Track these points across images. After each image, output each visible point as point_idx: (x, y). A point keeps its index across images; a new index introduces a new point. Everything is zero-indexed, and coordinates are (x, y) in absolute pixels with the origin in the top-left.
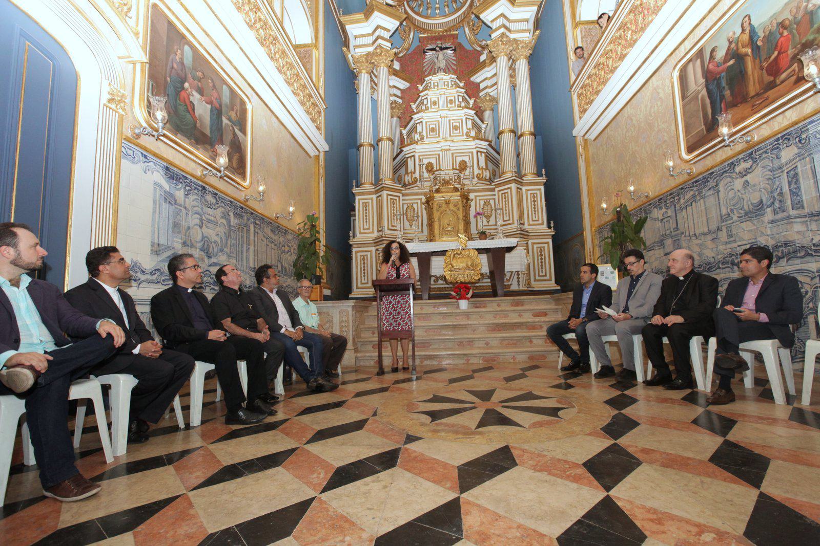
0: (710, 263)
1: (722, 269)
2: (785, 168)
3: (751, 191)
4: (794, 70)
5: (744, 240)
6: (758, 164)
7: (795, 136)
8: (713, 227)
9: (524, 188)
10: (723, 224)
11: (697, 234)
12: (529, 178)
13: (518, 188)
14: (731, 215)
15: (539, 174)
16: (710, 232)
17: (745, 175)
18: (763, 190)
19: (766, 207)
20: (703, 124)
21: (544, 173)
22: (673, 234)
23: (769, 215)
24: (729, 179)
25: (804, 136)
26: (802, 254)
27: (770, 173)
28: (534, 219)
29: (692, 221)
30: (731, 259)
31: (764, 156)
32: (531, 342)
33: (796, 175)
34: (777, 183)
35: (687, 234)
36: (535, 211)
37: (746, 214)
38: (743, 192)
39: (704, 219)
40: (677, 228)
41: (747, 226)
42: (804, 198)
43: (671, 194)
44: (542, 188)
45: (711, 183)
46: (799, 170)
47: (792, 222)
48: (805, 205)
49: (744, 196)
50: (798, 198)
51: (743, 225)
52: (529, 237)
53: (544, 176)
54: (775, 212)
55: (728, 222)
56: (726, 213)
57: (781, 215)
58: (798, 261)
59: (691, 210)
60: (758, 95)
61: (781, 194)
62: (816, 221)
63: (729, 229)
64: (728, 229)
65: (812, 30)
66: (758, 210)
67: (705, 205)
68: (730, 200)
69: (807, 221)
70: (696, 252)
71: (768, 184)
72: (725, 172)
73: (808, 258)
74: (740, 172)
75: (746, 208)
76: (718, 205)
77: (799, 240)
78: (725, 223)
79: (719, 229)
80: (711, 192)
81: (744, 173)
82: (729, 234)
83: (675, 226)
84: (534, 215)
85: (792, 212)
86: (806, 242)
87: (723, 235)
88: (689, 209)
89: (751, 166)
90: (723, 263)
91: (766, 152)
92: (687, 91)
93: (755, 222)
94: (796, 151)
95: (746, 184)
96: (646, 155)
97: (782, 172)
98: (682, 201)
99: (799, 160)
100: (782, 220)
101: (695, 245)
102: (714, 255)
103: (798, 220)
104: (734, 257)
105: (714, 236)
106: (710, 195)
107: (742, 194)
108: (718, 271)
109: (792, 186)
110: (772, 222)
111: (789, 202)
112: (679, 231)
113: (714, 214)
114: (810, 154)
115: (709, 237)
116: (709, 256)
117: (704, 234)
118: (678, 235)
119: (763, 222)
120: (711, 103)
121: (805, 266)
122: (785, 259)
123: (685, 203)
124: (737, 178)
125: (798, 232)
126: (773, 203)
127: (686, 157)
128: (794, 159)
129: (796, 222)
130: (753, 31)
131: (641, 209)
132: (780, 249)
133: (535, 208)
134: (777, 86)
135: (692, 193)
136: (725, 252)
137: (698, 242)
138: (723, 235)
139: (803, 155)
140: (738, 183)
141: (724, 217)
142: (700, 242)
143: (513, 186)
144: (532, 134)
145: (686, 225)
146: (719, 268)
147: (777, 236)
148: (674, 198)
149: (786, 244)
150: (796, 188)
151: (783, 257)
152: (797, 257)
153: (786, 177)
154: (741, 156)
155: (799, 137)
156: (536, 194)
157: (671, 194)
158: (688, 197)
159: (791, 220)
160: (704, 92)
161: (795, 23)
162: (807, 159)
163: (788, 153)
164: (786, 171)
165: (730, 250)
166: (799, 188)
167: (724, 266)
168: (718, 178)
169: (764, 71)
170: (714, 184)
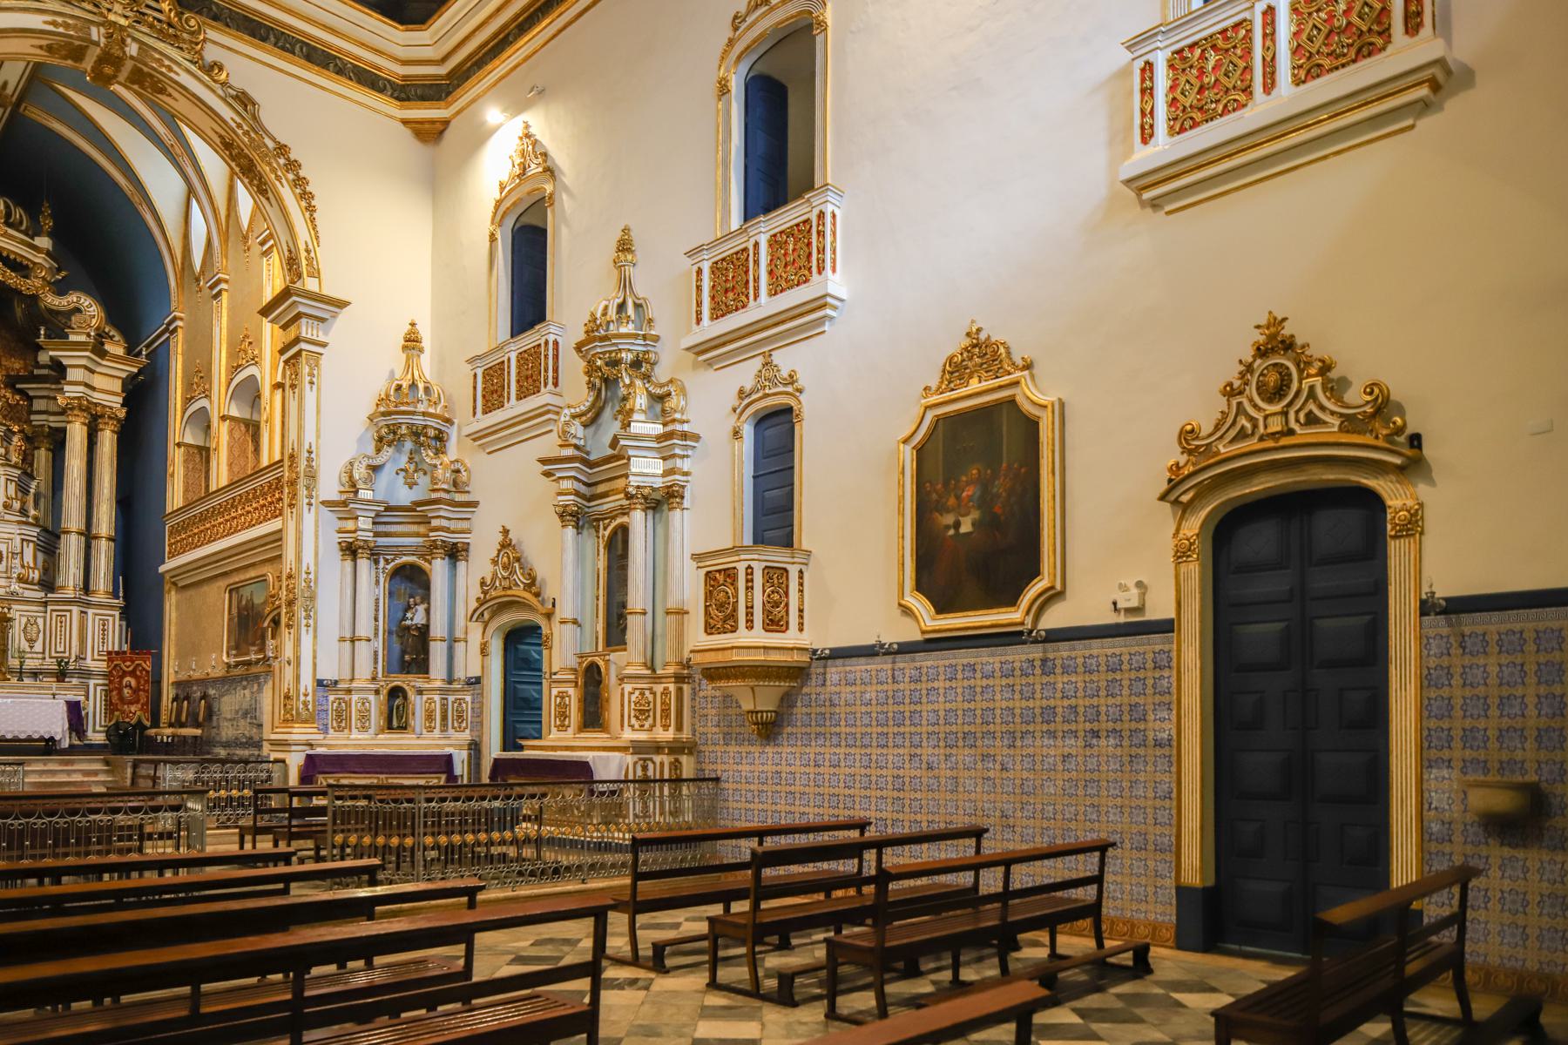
9: (90, 612)
12: (100, 597)
13: (82, 612)
36: (103, 643)
44: (117, 614)
133: (103, 639)
143: (75, 610)
144: (110, 539)
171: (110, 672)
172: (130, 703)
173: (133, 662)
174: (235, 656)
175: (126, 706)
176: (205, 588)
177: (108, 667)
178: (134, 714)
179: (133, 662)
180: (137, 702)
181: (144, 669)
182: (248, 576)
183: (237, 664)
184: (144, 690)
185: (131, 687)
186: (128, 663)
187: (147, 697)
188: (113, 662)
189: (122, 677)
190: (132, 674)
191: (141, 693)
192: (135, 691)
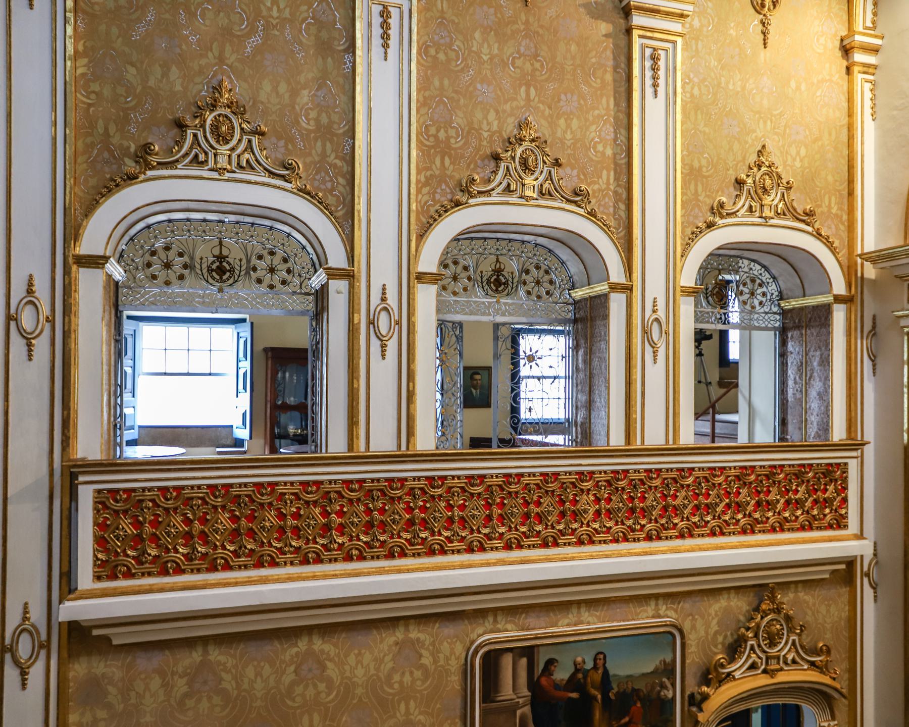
130: (606, 672)
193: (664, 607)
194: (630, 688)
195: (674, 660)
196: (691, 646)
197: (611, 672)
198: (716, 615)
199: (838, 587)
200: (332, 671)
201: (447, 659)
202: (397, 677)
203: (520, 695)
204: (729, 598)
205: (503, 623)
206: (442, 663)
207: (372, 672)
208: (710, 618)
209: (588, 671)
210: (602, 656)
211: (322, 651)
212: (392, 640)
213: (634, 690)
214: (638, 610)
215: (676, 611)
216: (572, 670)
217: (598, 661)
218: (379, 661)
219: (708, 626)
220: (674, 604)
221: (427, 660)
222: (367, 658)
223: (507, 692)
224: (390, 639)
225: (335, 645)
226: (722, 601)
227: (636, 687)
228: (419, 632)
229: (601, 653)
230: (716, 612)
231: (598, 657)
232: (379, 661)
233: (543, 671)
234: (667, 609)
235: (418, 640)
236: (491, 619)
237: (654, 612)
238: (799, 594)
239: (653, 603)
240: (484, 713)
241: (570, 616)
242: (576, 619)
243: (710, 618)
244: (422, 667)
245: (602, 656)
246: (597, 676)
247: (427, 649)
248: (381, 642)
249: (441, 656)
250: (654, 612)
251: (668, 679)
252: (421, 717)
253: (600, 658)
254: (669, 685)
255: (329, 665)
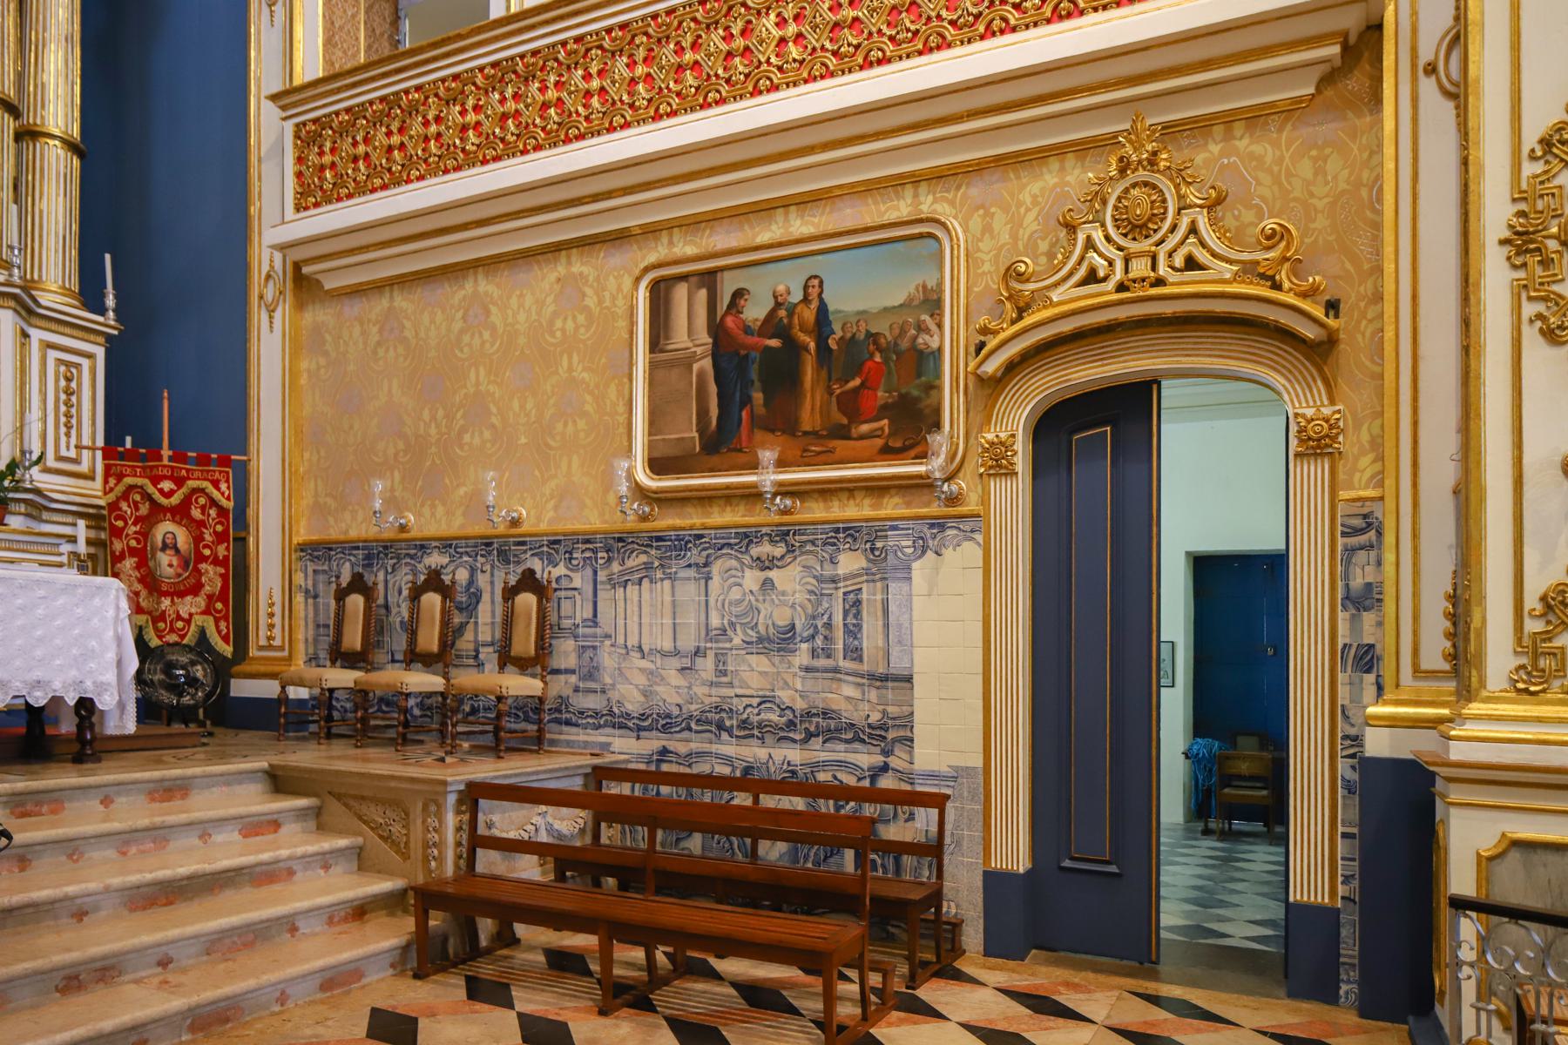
0: (668, 716)
1: (697, 732)
2: (841, 584)
3: (777, 602)
4: (882, 429)
5: (749, 687)
6: (795, 558)
7: (866, 538)
8: (688, 642)
10: (709, 645)
11: (646, 648)
14: (729, 632)
15: (90, 296)
16: (676, 653)
17: (768, 568)
18: (799, 608)
19: (799, 639)
20: (694, 428)
21: (110, 301)
22: (581, 631)
23: (802, 656)
24: (734, 563)
25: (879, 545)
26: (850, 735)
27: (814, 582)
28: (64, 453)
29: (636, 619)
30: (717, 717)
31: (809, 547)
32: (293, 929)
33: (858, 603)
34: (826, 605)
35: (621, 640)
36: (68, 427)
37: (760, 640)
38: (761, 598)
39: (668, 621)
40: (594, 621)
41: (760, 663)
42: (865, 645)
43: (588, 541)
44: (100, 352)
45: (694, 555)
46: (864, 596)
47: (840, 680)
48: (865, 658)
49: (760, 606)
50: (856, 643)
51: (753, 659)
52: (45, 515)
53: (111, 314)
54: (814, 653)
55: (721, 645)
56: (719, 626)
57: (822, 662)
58: (842, 747)
59: (636, 592)
60: (815, 434)
61: (828, 625)
62: (878, 688)
63: (720, 658)
64: (721, 657)
65: (917, 381)
66: (784, 640)
67: (673, 595)
68: (730, 604)
69: (863, 685)
70: (637, 686)
71: (809, 600)
72: (729, 545)
73: (857, 745)
74: (758, 559)
75: (761, 628)
76: (703, 604)
77: (851, 714)
78: (714, 645)
79: (698, 652)
80: (692, 573)
81: (767, 563)
82: (721, 667)
83: (588, 614)
84: (63, 439)
85: (842, 663)
86: (857, 717)
87: (707, 665)
88: (632, 590)
89: (783, 557)
90: (698, 721)
91: (813, 543)
92: (667, 337)
93: (777, 660)
94: (864, 564)
95: (767, 585)
96: (523, 420)
97: (837, 589)
98: (616, 567)
99: (867, 581)
100: (826, 670)
101: (636, 672)
102: (680, 701)
103: (850, 678)
104: (724, 715)
105: (687, 662)
106: (689, 579)
107: (757, 600)
108: (686, 734)
109: (848, 621)
110: (808, 669)
111: (840, 646)
112: (598, 630)
113: (690, 619)
114: (885, 579)
115: (676, 663)
116: (668, 700)
117: (664, 654)
118: (595, 636)
119: (790, 665)
120: (720, 396)
121: (851, 757)
122: (820, 739)
123: (622, 574)
124: (751, 568)
125: (848, 698)
126: (813, 637)
127: (644, 478)
128: (860, 575)
129: (848, 682)
131: (490, 544)
132: (815, 720)
133: (68, 416)
134: (848, 438)
135: (643, 558)
136: (707, 701)
137: (644, 664)
138: (707, 665)
139: (874, 574)
140: (752, 579)
141: (714, 632)
142: (652, 666)
145: (621, 622)
146: (690, 729)
147: (813, 695)
148: (595, 551)
149: (825, 714)
150: (854, 625)
151: (818, 735)
152: (840, 740)
153: (841, 600)
154: (764, 530)
155: (873, 542)
156: (78, 366)
157: (588, 541)
158: (635, 563)
159: (839, 676)
160: (707, 363)
161: (895, 352)
162: (879, 584)
163: (850, 562)
164: (842, 590)
165: (718, 700)
166: (859, 626)
167: (700, 728)
168: (710, 551)
169: (834, 399)
170: (702, 561)
171: (113, 506)
172: (179, 593)
173: (180, 482)
174: (782, 464)
175: (166, 602)
176: (484, 285)
177: (105, 493)
178: (188, 622)
179: (180, 482)
180: (195, 590)
181: (213, 503)
182: (764, 237)
183: (785, 490)
184: (216, 562)
185: (177, 551)
186: (167, 485)
187: (224, 577)
188: (120, 477)
189: (147, 523)
190: (180, 513)
191: (203, 566)
192: (192, 562)
193: (930, 198)
194: (864, 331)
195: (940, 284)
196: (983, 262)
197: (831, 308)
198: (1035, 202)
199: (1350, 114)
200: (496, 317)
201: (614, 298)
202: (559, 324)
203: (697, 342)
204: (1062, 169)
205: (681, 245)
206: (607, 303)
207: (534, 317)
208: (1022, 210)
209: (796, 305)
210: (816, 282)
211: (486, 293)
212: (553, 277)
213: (869, 335)
214: (883, 208)
215: (952, 203)
216: (770, 304)
217: (810, 290)
218: (540, 304)
219: (1016, 224)
220: (948, 191)
221: (591, 302)
222: (529, 300)
223: (680, 337)
224: (548, 276)
225: (498, 286)
226: (1047, 177)
227: (874, 331)
228: (582, 264)
229: (816, 277)
230: (1034, 197)
231: (810, 284)
232: (540, 304)
233: (730, 306)
234: (935, 201)
235: (581, 274)
236: (665, 240)
237: (910, 209)
238: (1237, 143)
239: (908, 192)
240: (653, 367)
241: (774, 227)
242: (782, 231)
243: (1022, 210)
244: (586, 309)
245: (816, 282)
246: (809, 314)
247: (591, 286)
248: (543, 279)
249: (607, 294)
250: (910, 209)
251: (932, 316)
252: (585, 375)
253: (814, 285)
254: (933, 327)
255: (493, 309)
